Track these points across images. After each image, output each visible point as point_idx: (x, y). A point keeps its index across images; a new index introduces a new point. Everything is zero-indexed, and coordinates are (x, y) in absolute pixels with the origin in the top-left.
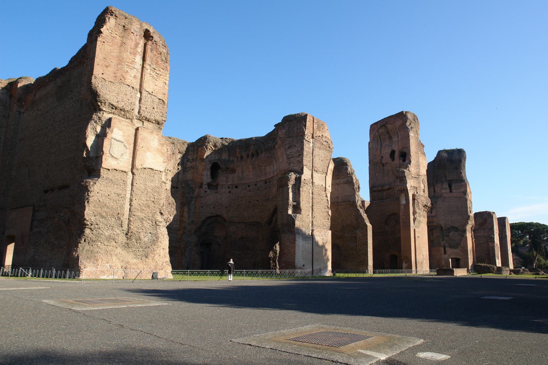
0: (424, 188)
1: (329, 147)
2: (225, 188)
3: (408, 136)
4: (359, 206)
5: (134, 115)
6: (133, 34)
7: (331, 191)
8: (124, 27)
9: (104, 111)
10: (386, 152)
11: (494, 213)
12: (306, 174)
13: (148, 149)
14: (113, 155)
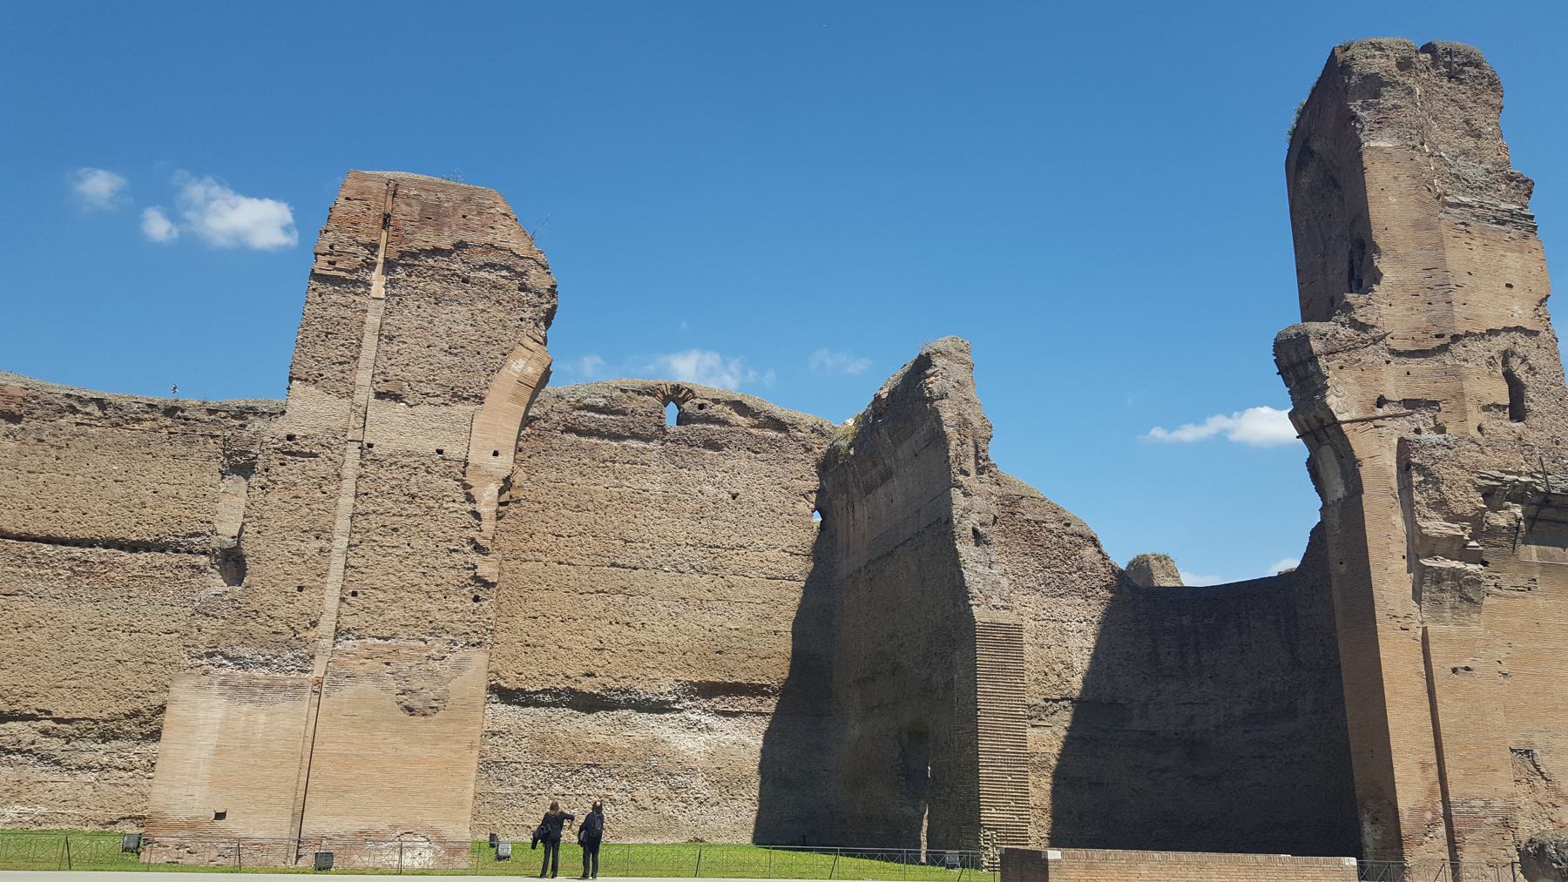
4: (975, 531)
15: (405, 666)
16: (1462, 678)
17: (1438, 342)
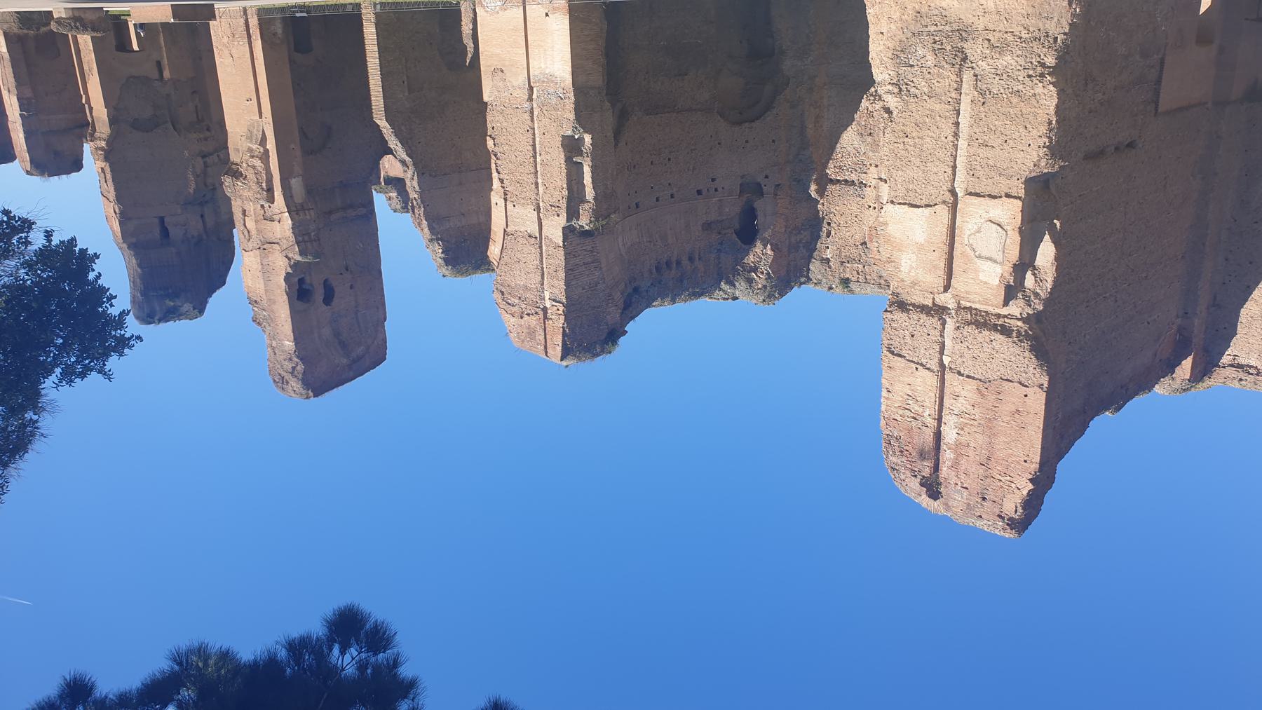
0: (244, 220)
1: (502, 293)
2: (723, 188)
3: (296, 340)
4: (408, 169)
5: (954, 316)
6: (965, 486)
7: (492, 193)
8: (984, 499)
9: (1018, 319)
10: (343, 299)
11: (28, 173)
12: (555, 229)
13: (921, 248)
14: (999, 228)
15: (506, 93)
16: (248, 97)
17: (265, 246)
